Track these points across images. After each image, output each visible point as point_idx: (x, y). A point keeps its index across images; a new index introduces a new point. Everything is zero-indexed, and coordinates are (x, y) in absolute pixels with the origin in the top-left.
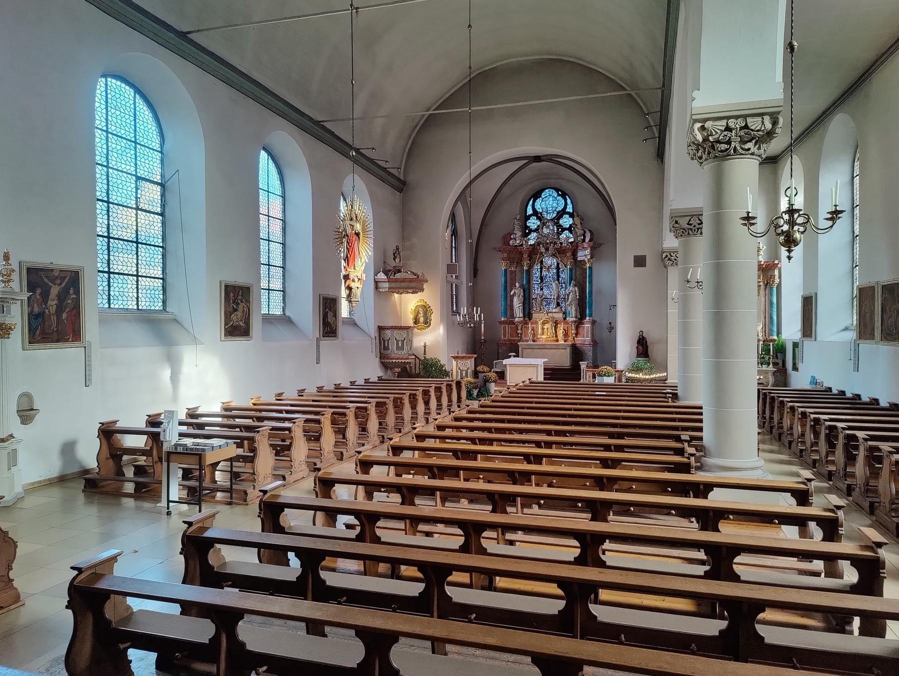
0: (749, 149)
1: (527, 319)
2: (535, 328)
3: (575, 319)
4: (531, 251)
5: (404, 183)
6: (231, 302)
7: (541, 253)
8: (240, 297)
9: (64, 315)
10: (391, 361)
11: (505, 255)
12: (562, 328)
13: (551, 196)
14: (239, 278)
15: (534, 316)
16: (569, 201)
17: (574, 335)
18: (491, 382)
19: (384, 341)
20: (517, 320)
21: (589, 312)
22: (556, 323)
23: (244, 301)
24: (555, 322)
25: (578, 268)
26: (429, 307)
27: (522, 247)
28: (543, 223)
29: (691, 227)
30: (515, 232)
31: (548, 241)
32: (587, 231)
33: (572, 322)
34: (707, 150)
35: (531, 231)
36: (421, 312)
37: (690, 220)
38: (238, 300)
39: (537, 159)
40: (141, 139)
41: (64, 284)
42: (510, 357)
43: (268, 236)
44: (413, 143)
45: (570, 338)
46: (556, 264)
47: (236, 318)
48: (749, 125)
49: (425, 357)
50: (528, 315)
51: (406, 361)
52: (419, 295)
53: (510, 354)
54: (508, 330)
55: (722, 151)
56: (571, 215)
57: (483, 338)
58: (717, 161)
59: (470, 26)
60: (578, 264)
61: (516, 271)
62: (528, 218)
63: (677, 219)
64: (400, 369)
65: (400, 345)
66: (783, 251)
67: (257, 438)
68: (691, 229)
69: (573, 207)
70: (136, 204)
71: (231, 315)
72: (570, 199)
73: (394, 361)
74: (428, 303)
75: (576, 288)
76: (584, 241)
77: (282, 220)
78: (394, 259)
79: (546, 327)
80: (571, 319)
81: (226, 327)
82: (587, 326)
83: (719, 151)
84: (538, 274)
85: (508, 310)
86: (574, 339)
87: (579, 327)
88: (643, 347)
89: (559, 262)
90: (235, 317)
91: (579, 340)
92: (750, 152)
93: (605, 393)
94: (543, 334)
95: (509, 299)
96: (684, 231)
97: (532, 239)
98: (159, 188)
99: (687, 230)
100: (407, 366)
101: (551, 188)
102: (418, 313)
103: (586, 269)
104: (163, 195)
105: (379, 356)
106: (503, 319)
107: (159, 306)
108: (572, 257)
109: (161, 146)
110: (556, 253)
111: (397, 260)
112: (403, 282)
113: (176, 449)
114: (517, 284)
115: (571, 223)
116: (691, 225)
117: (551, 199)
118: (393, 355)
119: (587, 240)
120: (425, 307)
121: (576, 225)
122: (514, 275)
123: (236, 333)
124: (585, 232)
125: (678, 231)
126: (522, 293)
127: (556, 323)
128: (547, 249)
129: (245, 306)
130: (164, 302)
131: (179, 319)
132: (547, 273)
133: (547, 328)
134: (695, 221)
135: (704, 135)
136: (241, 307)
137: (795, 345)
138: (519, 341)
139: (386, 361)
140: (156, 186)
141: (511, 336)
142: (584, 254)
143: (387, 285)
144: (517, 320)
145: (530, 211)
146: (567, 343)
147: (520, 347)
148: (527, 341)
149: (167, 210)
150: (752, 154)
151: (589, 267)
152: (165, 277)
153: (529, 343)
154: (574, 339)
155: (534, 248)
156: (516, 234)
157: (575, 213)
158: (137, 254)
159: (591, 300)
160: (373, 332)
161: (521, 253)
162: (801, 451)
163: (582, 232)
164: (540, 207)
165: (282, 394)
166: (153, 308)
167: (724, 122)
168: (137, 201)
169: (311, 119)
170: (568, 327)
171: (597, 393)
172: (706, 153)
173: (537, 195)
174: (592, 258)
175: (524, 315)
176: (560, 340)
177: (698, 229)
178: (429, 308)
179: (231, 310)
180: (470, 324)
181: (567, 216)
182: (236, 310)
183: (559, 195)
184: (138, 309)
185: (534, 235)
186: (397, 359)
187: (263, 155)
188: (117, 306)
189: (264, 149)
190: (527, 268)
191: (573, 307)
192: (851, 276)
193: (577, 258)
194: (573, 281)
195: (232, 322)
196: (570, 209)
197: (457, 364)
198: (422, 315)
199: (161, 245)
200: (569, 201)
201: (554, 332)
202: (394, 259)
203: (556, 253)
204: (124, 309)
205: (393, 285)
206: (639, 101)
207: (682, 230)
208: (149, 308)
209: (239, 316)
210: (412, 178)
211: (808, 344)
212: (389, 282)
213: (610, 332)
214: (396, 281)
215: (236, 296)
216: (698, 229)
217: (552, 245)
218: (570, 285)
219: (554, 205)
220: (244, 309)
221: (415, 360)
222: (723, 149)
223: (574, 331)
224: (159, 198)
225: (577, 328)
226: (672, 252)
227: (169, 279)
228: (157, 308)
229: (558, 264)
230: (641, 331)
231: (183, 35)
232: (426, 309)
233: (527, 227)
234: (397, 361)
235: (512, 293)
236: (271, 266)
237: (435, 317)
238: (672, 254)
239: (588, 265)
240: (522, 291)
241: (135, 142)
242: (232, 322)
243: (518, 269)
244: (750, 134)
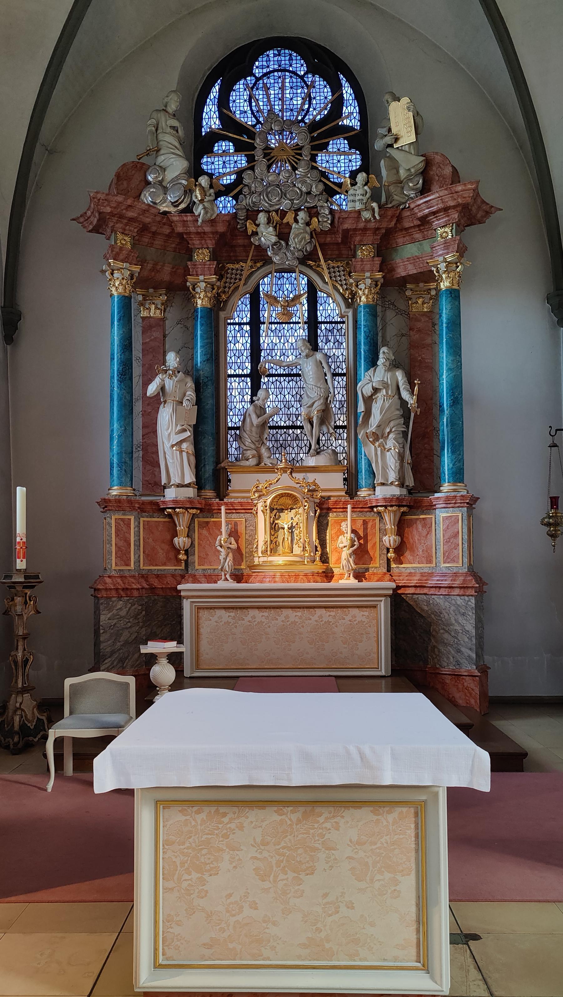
1: (209, 493)
2: (241, 529)
7: (261, 251)
12: (346, 526)
13: (285, 70)
16: (347, 91)
17: (391, 555)
20: (170, 494)
27: (189, 218)
31: (285, 205)
33: (389, 502)
54: (138, 534)
57: (21, 564)
61: (163, 320)
79: (286, 519)
80: (381, 492)
85: (138, 464)
86: (389, 570)
87: (411, 523)
95: (138, 407)
106: (115, 491)
108: (378, 261)
114: (172, 359)
122: (157, 334)
126: (191, 394)
138: (182, 578)
141: (151, 558)
144: (170, 494)
146: (365, 584)
148: (212, 578)
153: (221, 584)
154: (389, 570)
164: (247, 108)
170: (365, 523)
175: (198, 476)
176: (336, 571)
181: (341, 144)
183: (311, 70)
194: (384, 349)
200: (347, 91)
201: (317, 543)
213: (553, 536)
217: (302, 215)
218: (373, 363)
223: (390, 540)
235: (152, 389)
239: (444, 285)
240: (190, 384)
243: (173, 315)
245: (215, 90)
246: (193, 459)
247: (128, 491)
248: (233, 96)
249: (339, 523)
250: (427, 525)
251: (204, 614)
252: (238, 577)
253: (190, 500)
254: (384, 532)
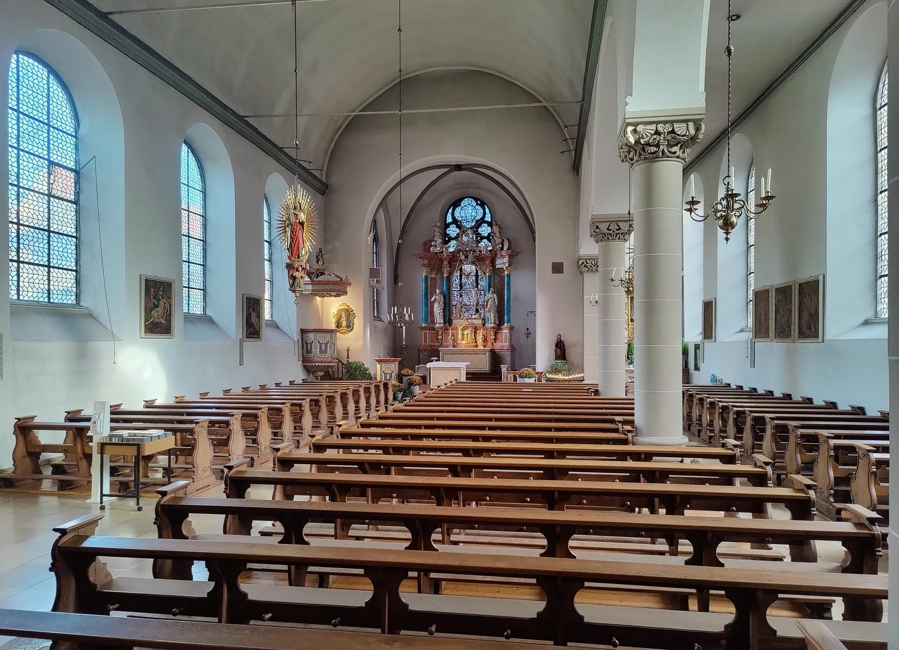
0: (675, 153)
1: (447, 325)
2: (455, 334)
3: (493, 325)
4: (451, 258)
5: (326, 186)
6: (152, 297)
7: (461, 260)
8: (161, 293)
10: (314, 364)
11: (426, 262)
12: (481, 334)
14: (161, 273)
15: (454, 322)
16: (487, 210)
18: (415, 385)
19: (307, 344)
20: (437, 325)
21: (507, 318)
22: (476, 329)
24: (475, 328)
25: (496, 276)
26: (353, 311)
28: (463, 231)
29: (611, 232)
30: (435, 239)
31: (468, 249)
32: (505, 240)
33: (491, 328)
34: (638, 152)
35: (451, 239)
36: (344, 316)
37: (609, 226)
38: (158, 296)
39: (458, 167)
40: (55, 122)
42: (432, 361)
43: (188, 232)
44: (335, 146)
45: (489, 344)
46: (475, 271)
47: (157, 314)
48: (676, 130)
49: (348, 361)
50: (448, 321)
51: (330, 364)
52: (343, 298)
53: (432, 358)
55: (652, 153)
56: (490, 224)
57: (404, 343)
58: (646, 163)
59: (400, 29)
60: (496, 272)
61: (436, 278)
62: (447, 226)
63: (598, 224)
64: (323, 373)
65: (323, 348)
66: (721, 233)
67: (196, 429)
68: (611, 234)
69: (491, 216)
70: (49, 190)
71: (152, 311)
72: (489, 209)
73: (317, 364)
74: (350, 307)
75: (495, 295)
76: (502, 249)
77: (203, 216)
78: (318, 262)
79: (466, 332)
80: (490, 325)
81: (147, 323)
82: (505, 331)
83: (649, 154)
84: (457, 281)
85: (429, 316)
86: (493, 345)
87: (498, 333)
88: (560, 350)
89: (478, 269)
90: (156, 314)
91: (498, 346)
92: (676, 155)
93: (532, 390)
94: (463, 340)
95: (429, 305)
96: (604, 236)
97: (452, 246)
98: (73, 175)
99: (607, 235)
100: (330, 370)
101: (470, 197)
102: (341, 317)
103: (505, 276)
104: (77, 182)
105: (301, 359)
107: (72, 300)
109: (75, 129)
110: (475, 261)
111: (320, 263)
112: (326, 284)
113: (111, 439)
114: (438, 291)
115: (489, 231)
116: (610, 230)
117: (470, 208)
118: (316, 359)
119: (505, 248)
120: (347, 310)
121: (495, 234)
122: (434, 281)
123: (157, 330)
124: (503, 240)
125: (598, 236)
127: (476, 329)
128: (467, 257)
129: (166, 302)
130: (78, 296)
131: (95, 315)
132: (467, 281)
133: (467, 334)
134: (614, 227)
135: (636, 137)
136: (162, 303)
137: (697, 347)
139: (308, 364)
140: (70, 172)
142: (502, 262)
143: (310, 287)
144: (437, 325)
145: (449, 219)
146: (486, 348)
147: (441, 353)
148: (447, 347)
149: (81, 197)
150: (678, 157)
151: (507, 275)
152: (78, 269)
153: (449, 348)
154: (493, 345)
155: (454, 256)
156: (436, 241)
157: (493, 222)
158: (49, 243)
159: (509, 306)
160: (296, 336)
161: (441, 260)
162: (710, 437)
163: (500, 240)
165: (207, 393)
166: (65, 302)
167: (653, 127)
168: (49, 187)
169: (234, 113)
170: (487, 333)
171: (523, 390)
172: (637, 155)
173: (456, 204)
174: (510, 265)
175: (444, 321)
176: (479, 345)
177: (617, 234)
178: (351, 312)
180: (401, 324)
181: (486, 225)
182: (156, 306)
183: (478, 204)
184: (49, 302)
185: (453, 243)
186: (321, 362)
187: (184, 148)
188: (26, 298)
189: (186, 142)
190: (447, 275)
191: (492, 313)
192: (745, 282)
193: (495, 266)
194: (491, 288)
195: (153, 318)
196: (488, 218)
197: (381, 367)
198: (345, 318)
199: (74, 234)
200: (487, 210)
201: (473, 338)
202: (318, 262)
203: (475, 261)
204: (35, 301)
205: (317, 287)
206: (556, 116)
207: (602, 235)
208: (61, 301)
209: (160, 313)
210: (335, 180)
211: (708, 345)
212: (312, 284)
213: (527, 337)
214: (320, 283)
216: (617, 234)
217: (471, 252)
219: (473, 214)
220: (165, 306)
221: (338, 364)
222: (652, 151)
223: (492, 337)
224: (73, 185)
225: (496, 334)
226: (588, 259)
227: (83, 272)
228: (70, 302)
229: (477, 271)
230: (559, 335)
231: (105, 16)
232: (349, 313)
233: (446, 235)
234: (320, 364)
235: (433, 299)
236: (191, 263)
237: (358, 322)
238: (588, 261)
240: (442, 297)
241: (48, 125)
242: (153, 318)
243: (438, 276)
244: (676, 139)
245: (450, 211)
246: (443, 317)
247: (427, 325)
248: (455, 212)
249: (479, 333)
250: (502, 333)
251: (445, 355)
252: (454, 347)
253: (442, 327)
254: (491, 335)
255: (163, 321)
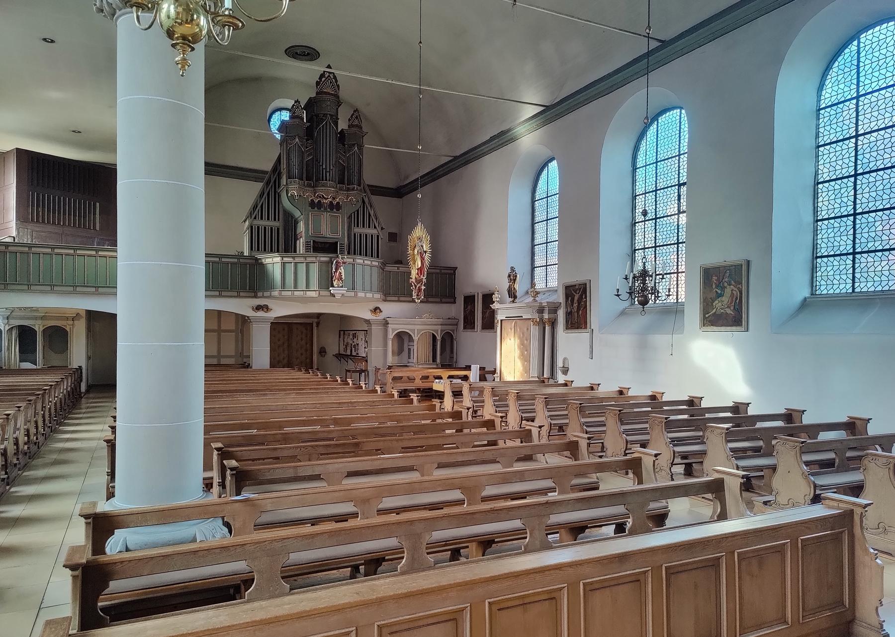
9: (580, 312)
23: (733, 283)
38: (723, 284)
41: (580, 293)
81: (707, 316)
90: (720, 304)
136: (728, 291)
179: (714, 295)
182: (720, 295)
209: (725, 302)
215: (721, 278)
255: (729, 311)
